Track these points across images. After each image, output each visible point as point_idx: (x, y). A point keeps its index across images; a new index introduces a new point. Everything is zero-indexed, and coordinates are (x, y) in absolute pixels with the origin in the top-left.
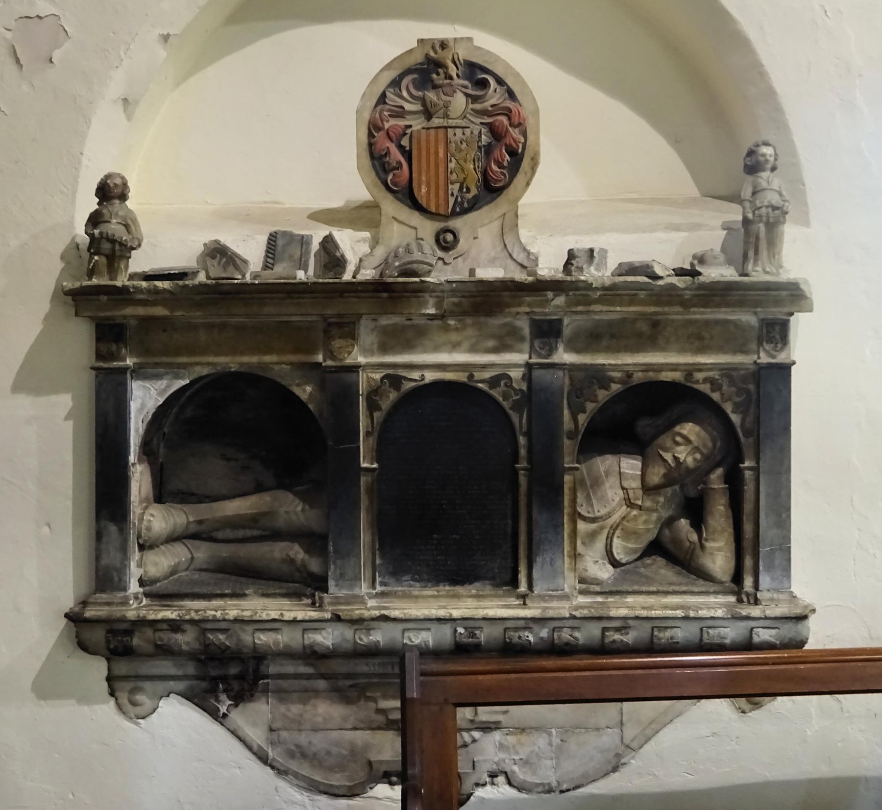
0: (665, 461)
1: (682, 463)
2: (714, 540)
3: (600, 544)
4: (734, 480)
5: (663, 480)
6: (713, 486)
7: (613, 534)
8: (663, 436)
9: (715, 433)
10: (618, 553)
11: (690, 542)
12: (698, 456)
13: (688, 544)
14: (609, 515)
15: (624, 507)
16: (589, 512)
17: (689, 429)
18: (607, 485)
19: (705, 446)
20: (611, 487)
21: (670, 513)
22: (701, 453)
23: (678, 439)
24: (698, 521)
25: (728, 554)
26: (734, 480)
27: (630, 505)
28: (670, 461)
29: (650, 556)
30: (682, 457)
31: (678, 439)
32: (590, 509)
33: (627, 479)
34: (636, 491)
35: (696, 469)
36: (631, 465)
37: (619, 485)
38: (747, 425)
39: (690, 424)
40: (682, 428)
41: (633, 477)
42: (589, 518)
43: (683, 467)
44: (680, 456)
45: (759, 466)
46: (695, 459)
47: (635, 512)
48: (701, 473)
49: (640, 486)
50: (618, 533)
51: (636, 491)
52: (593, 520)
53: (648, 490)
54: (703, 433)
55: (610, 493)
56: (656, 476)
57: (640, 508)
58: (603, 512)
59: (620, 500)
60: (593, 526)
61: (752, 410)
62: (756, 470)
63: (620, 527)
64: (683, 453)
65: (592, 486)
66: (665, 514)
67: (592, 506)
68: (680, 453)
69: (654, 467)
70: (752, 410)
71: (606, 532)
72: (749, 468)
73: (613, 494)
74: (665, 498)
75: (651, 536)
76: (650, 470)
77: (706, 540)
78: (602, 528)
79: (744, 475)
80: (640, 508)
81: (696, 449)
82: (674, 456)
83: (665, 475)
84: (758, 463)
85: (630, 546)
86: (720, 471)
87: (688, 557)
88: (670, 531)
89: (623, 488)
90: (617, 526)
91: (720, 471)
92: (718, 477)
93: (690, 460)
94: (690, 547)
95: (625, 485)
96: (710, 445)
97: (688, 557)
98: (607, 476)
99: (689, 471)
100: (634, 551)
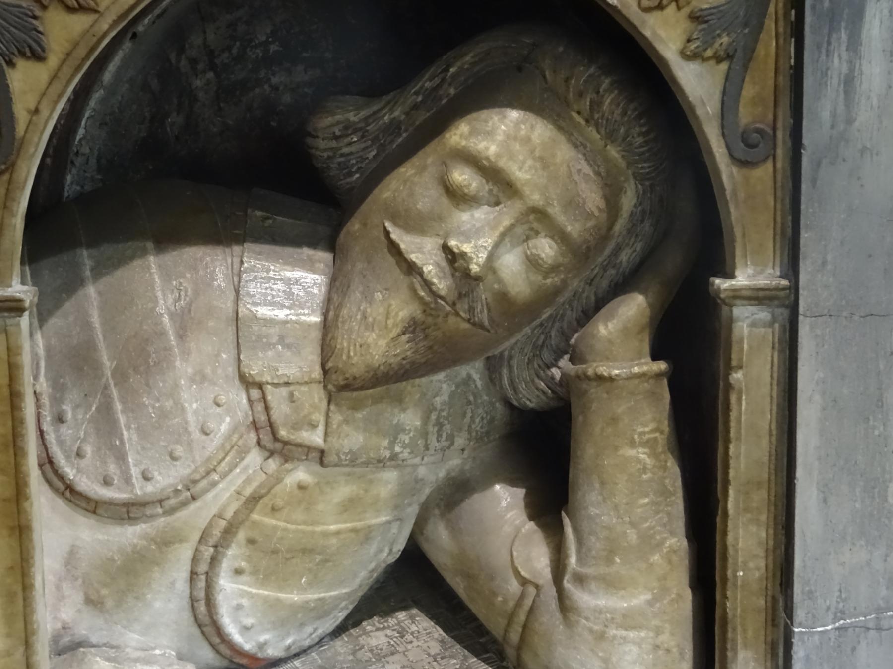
0: (411, 269)
1: (478, 279)
2: (611, 584)
3: (166, 599)
4: (690, 343)
5: (404, 349)
6: (603, 370)
7: (214, 561)
8: (406, 170)
9: (614, 152)
10: (245, 629)
11: (524, 582)
12: (546, 248)
13: (514, 587)
14: (190, 492)
15: (254, 458)
16: (107, 482)
17: (506, 134)
18: (183, 368)
19: (572, 204)
20: (200, 378)
21: (455, 462)
22: (560, 236)
23: (462, 176)
24: (551, 503)
25: (665, 638)
26: (690, 343)
27: (280, 448)
28: (429, 269)
29: (388, 612)
30: (476, 251)
31: (462, 176)
32: (112, 468)
33: (262, 343)
34: (300, 392)
35: (545, 298)
36: (283, 287)
37: (231, 370)
38: (745, 115)
39: (514, 114)
40: (474, 132)
41: (286, 336)
42: (110, 503)
43: (483, 294)
44: (467, 248)
45: (795, 288)
46: (533, 262)
47: (301, 474)
48: (561, 316)
49: (317, 373)
50: (234, 555)
51: (300, 392)
52: (128, 512)
53: (344, 386)
54: (564, 152)
55: (192, 405)
56: (379, 329)
57: (321, 457)
58: (165, 479)
59: (234, 429)
60: (130, 535)
61: (768, 46)
62: (786, 304)
63: (241, 535)
64: (478, 232)
65: (121, 376)
66: (432, 472)
67: (121, 458)
68: (467, 237)
69: (368, 297)
70: (768, 46)
71: (184, 553)
72: (758, 297)
73: (204, 405)
74: (429, 410)
75: (386, 550)
76: (352, 307)
77: (580, 580)
78: (166, 541)
79: (731, 320)
80: (321, 457)
81: (537, 219)
82: (446, 248)
83: (412, 327)
84: (792, 268)
85: (295, 597)
86: (634, 307)
87: (514, 637)
88: (455, 530)
89: (247, 382)
90: (229, 532)
91: (634, 307)
92: (625, 331)
93: (511, 263)
94: (523, 596)
95: (254, 370)
96: (593, 198)
97: (514, 637)
98: (181, 337)
99: (511, 312)
100: (320, 610)
